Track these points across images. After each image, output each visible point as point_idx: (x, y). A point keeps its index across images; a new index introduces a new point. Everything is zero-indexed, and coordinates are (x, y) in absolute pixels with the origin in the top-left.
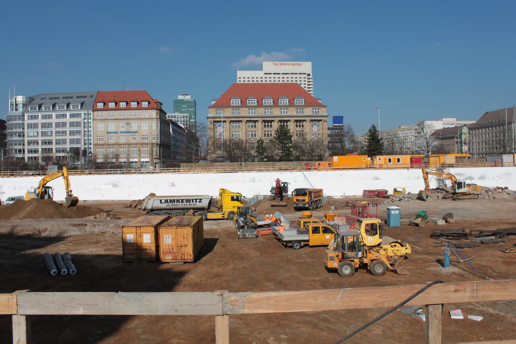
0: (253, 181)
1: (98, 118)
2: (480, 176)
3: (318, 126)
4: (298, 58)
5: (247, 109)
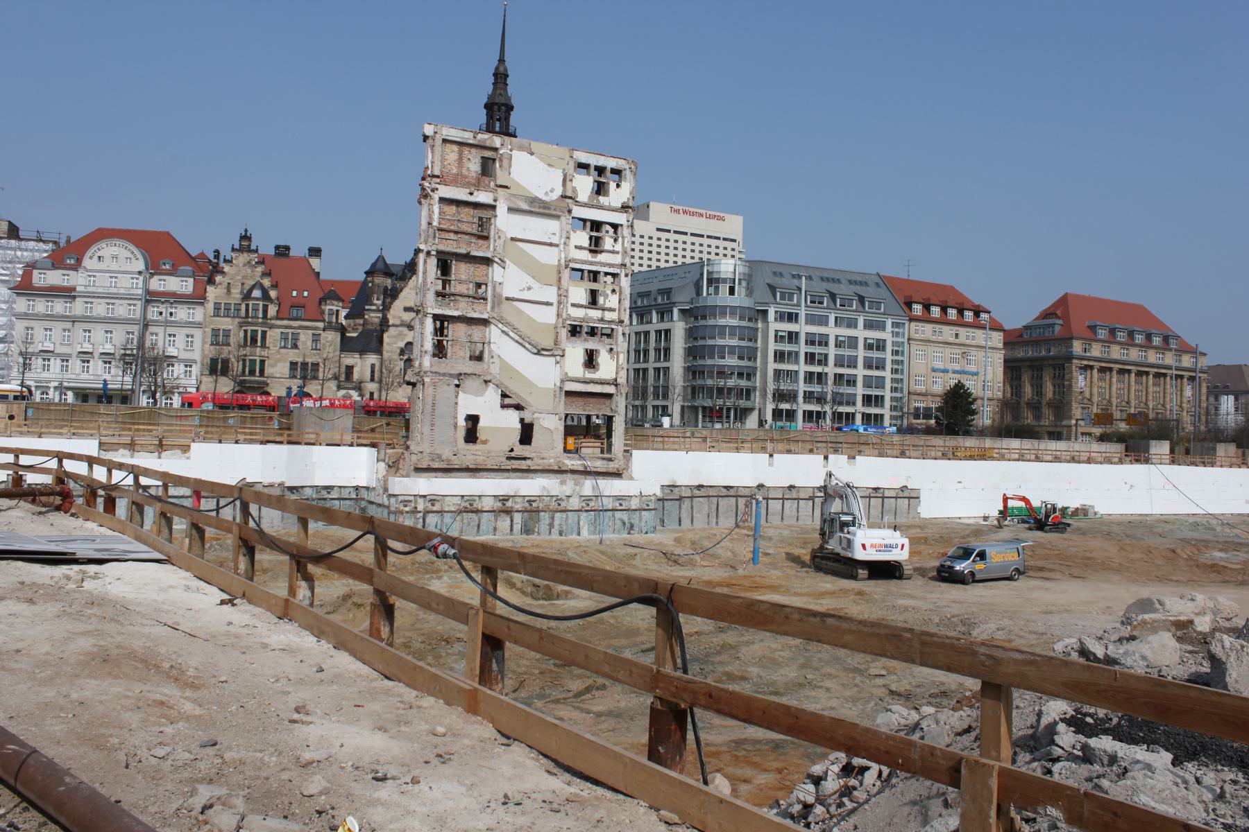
4: (718, 206)
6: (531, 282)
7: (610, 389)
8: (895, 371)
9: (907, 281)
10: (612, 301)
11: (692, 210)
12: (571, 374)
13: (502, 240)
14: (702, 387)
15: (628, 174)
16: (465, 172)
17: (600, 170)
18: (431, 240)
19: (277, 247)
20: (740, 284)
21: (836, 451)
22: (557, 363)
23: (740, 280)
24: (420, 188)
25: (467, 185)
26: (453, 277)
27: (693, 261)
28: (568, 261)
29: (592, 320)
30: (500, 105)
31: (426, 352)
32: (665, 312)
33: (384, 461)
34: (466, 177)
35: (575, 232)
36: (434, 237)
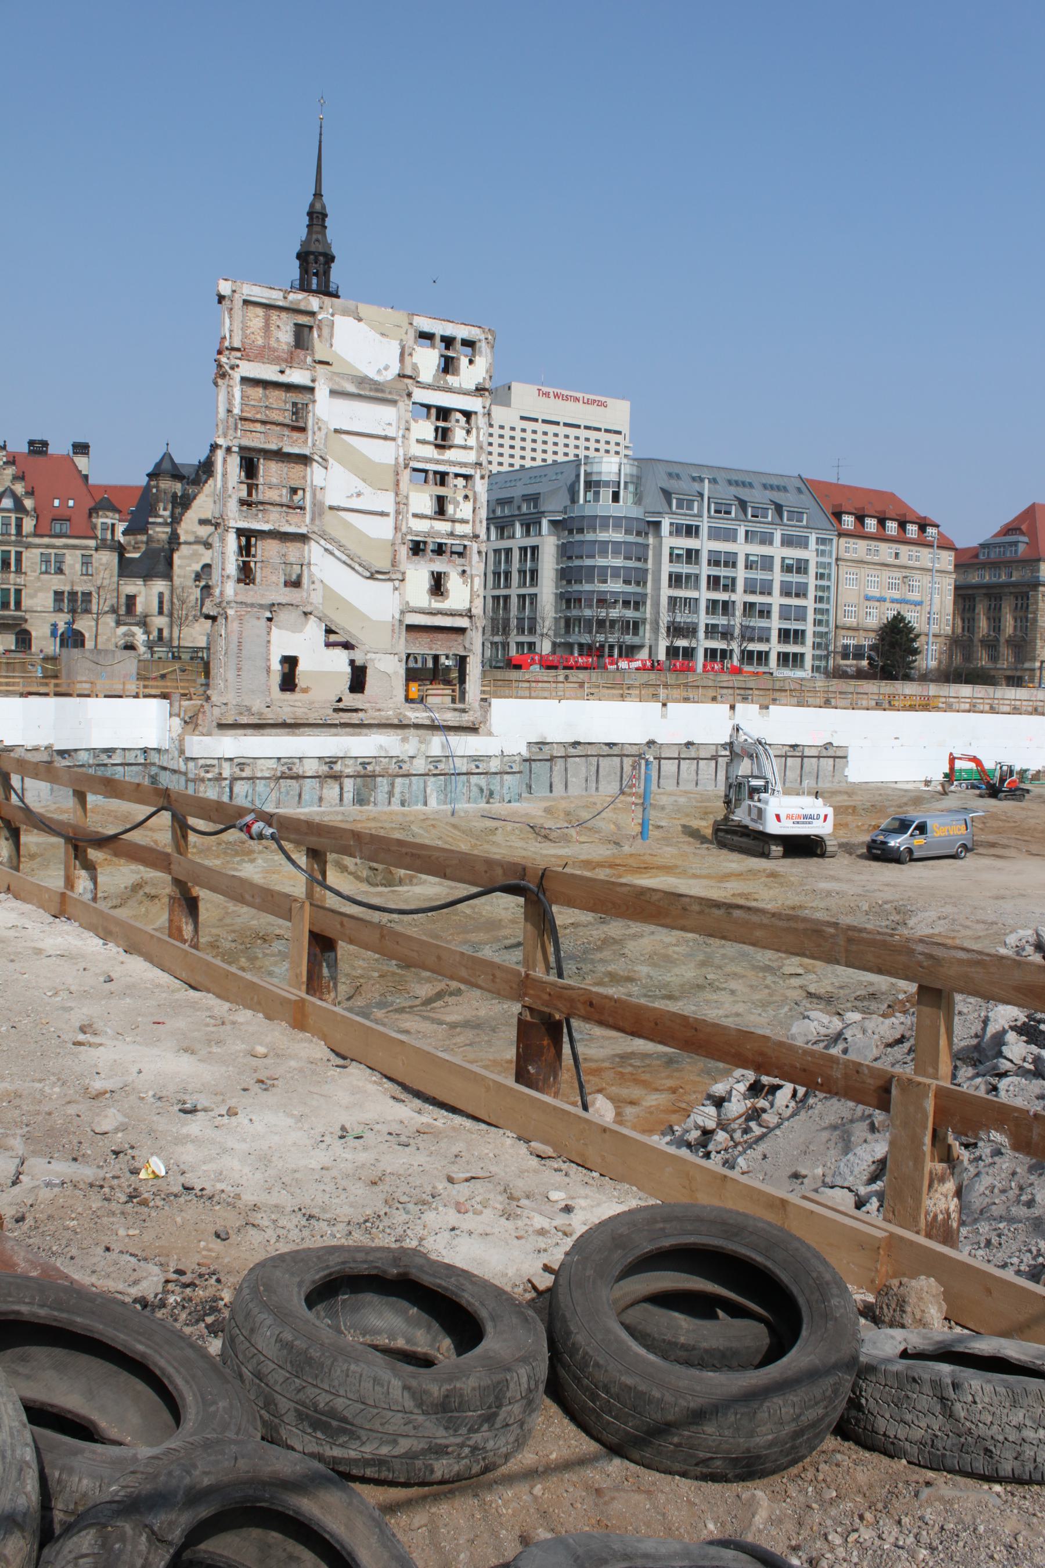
6: (361, 486)
7: (463, 622)
8: (819, 599)
9: (836, 485)
10: (464, 510)
11: (565, 393)
12: (414, 603)
13: (324, 432)
14: (579, 619)
15: (483, 346)
16: (273, 343)
17: (448, 342)
18: (231, 432)
19: (31, 443)
20: (626, 488)
21: (745, 699)
22: (396, 589)
23: (626, 483)
24: (215, 364)
25: (276, 360)
26: (261, 480)
27: (566, 459)
28: (408, 459)
29: (438, 534)
30: (317, 255)
31: (228, 577)
32: (531, 525)
33: (178, 715)
34: (275, 350)
35: (416, 421)
36: (236, 429)
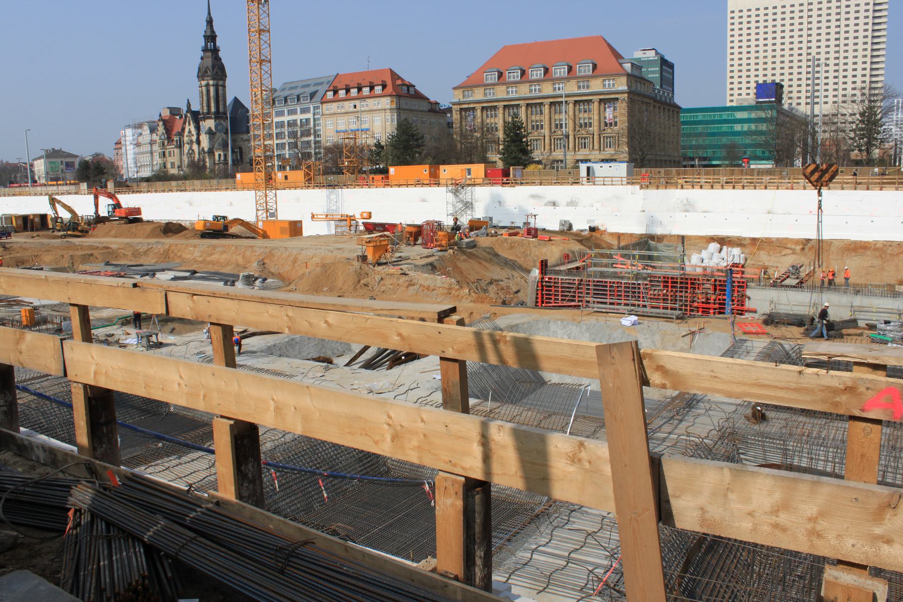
0: (298, 200)
1: (328, 112)
2: (569, 200)
3: (615, 109)
5: (504, 87)
9: (368, 72)
